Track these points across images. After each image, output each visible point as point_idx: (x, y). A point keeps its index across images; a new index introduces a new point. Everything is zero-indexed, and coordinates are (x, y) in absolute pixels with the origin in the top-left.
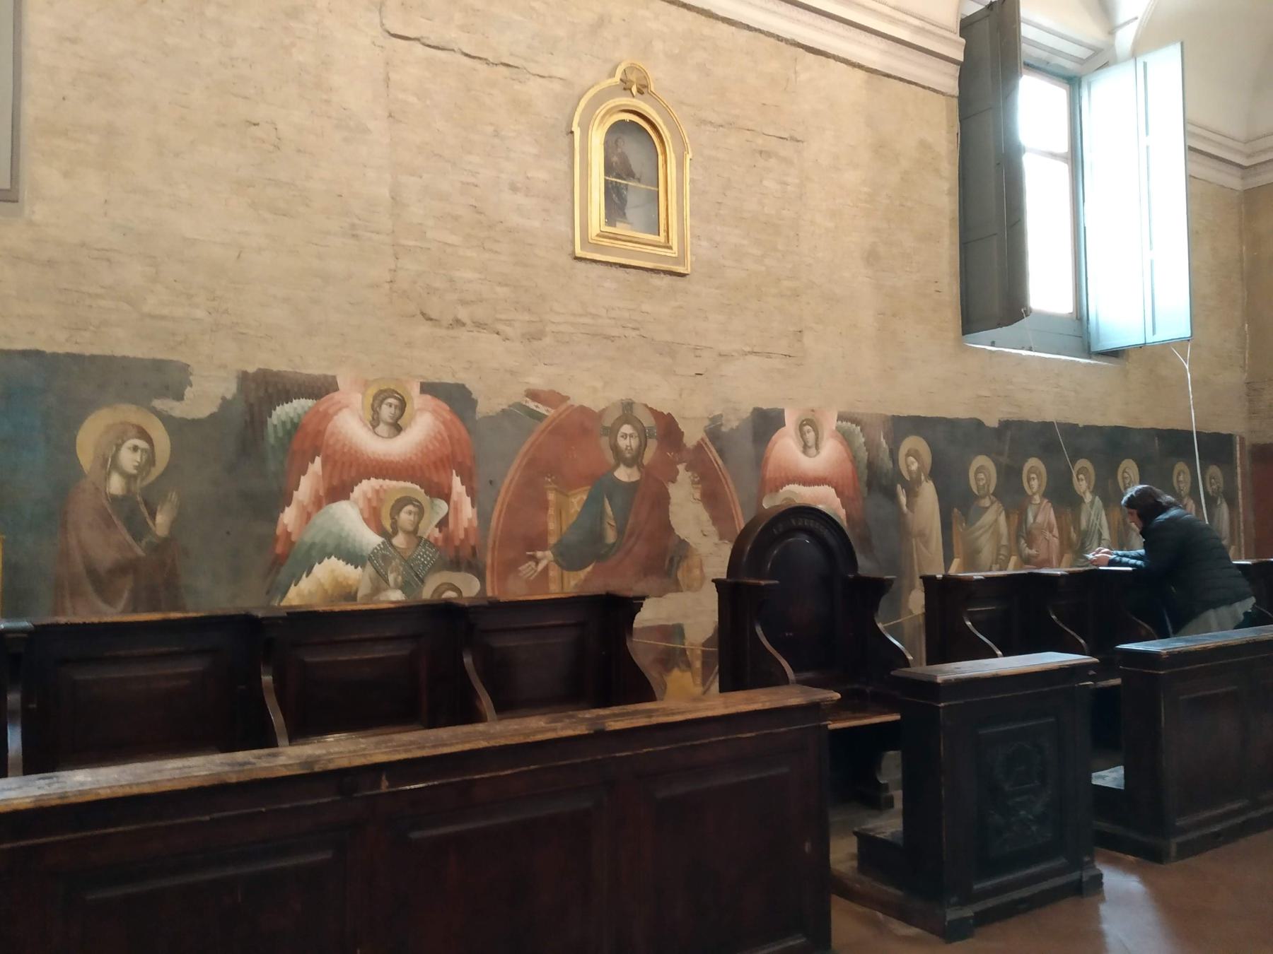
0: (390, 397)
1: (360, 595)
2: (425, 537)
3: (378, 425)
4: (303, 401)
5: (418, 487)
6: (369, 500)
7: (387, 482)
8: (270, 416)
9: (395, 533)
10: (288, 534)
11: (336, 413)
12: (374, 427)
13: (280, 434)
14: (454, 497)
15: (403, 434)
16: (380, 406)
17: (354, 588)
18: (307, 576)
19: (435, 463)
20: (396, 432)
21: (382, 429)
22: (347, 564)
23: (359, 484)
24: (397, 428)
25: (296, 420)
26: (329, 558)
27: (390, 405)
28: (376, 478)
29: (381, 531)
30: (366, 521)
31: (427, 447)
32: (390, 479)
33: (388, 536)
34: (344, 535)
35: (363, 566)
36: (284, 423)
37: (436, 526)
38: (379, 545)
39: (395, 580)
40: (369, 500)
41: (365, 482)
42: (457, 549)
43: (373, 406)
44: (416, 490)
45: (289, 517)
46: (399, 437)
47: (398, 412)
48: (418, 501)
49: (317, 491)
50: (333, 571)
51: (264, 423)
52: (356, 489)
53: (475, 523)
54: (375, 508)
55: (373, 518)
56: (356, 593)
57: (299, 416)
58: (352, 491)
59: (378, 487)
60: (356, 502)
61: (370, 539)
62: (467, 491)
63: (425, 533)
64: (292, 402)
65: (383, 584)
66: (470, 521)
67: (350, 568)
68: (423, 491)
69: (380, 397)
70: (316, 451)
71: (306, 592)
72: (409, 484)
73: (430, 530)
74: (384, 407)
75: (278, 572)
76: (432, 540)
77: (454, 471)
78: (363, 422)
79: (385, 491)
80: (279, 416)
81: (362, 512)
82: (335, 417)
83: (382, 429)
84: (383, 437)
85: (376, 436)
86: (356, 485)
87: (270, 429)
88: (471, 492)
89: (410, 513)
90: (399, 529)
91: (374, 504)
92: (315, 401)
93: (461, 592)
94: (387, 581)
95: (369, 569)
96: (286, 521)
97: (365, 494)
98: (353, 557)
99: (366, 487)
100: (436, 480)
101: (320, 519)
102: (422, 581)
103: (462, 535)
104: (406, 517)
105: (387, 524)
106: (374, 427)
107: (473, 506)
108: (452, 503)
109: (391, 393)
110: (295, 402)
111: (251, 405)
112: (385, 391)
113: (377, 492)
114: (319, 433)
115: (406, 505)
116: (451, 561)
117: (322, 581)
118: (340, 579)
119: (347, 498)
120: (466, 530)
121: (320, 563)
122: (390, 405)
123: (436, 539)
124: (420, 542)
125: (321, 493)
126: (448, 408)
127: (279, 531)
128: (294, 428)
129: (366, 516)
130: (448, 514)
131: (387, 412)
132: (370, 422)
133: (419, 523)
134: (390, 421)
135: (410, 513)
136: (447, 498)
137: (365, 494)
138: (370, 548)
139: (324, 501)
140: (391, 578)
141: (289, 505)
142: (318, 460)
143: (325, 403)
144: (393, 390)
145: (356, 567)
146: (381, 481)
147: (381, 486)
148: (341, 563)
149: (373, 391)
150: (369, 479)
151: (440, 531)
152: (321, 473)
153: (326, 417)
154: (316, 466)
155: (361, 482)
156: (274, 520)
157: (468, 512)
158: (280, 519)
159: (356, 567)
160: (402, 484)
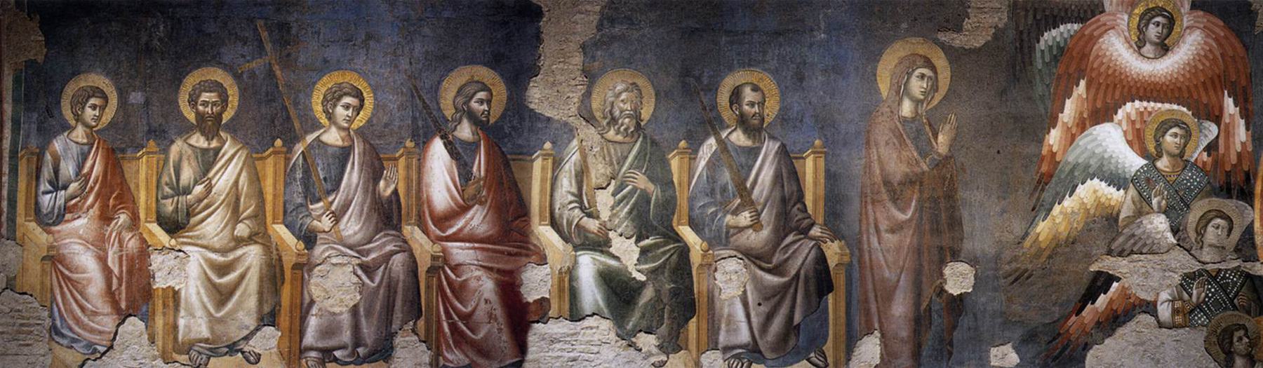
0: (1158, 15)
1: (1122, 216)
2: (1193, 160)
3: (1144, 45)
4: (1069, 26)
5: (1185, 109)
6: (1133, 122)
7: (1152, 104)
8: (1038, 42)
9: (1160, 156)
10: (1053, 155)
11: (1100, 36)
12: (1140, 48)
13: (1047, 60)
14: (1226, 119)
15: (1170, 53)
16: (1147, 25)
17: (1116, 209)
18: (1070, 196)
19: (1204, 83)
20: (1162, 53)
21: (1148, 49)
22: (1109, 185)
23: (1123, 107)
24: (1164, 48)
25: (1062, 45)
26: (1091, 179)
27: (1158, 24)
28: (1141, 100)
29: (1143, 153)
30: (1130, 143)
31: (1195, 67)
32: (1155, 101)
33: (1152, 159)
34: (1106, 156)
35: (1126, 189)
36: (1051, 48)
37: (1204, 150)
38: (1142, 167)
39: (1159, 203)
40: (1133, 122)
41: (1129, 105)
42: (1228, 174)
43: (1139, 25)
44: (1183, 112)
45: (1054, 138)
46: (1164, 57)
47: (1165, 31)
48: (1185, 124)
49: (1081, 113)
50: (1095, 191)
51: (1032, 49)
52: (1120, 111)
53: (1250, 149)
54: (1138, 130)
55: (1136, 140)
56: (1118, 215)
57: (1065, 40)
58: (1116, 114)
59: (1142, 110)
60: (1120, 123)
61: (1133, 162)
62: (1240, 112)
63: (1192, 157)
64: (1058, 27)
65: (1147, 208)
66: (1243, 144)
67: (1112, 190)
68: (1190, 113)
69: (1147, 17)
70: (1081, 74)
71: (1069, 210)
72: (1175, 107)
73: (1198, 153)
74: (1151, 26)
75: (1043, 190)
76: (1200, 165)
77: (1226, 92)
78: (1129, 43)
79: (1150, 113)
80: (1046, 41)
81: (1125, 133)
82: (1101, 40)
83: (1148, 49)
84: (1148, 58)
85: (1142, 58)
86: (1120, 108)
87: (1038, 55)
88: (1245, 114)
89: (1175, 135)
90: (1164, 152)
91: (1138, 126)
92: (1081, 25)
93: (1231, 221)
94: (1150, 204)
95: (1132, 191)
96: (1051, 143)
97: (1128, 116)
98: (1116, 180)
99: (1130, 108)
100: (1205, 100)
101: (1083, 141)
102: (1188, 207)
103: (1234, 160)
104: (1171, 140)
105: (1151, 147)
106: (1140, 48)
107: (1247, 129)
108: (1222, 126)
109: (1160, 11)
110: (1062, 28)
111: (1021, 32)
112: (1153, 9)
113: (1142, 113)
114: (1084, 56)
115: (1171, 128)
116: (1221, 188)
117: (1085, 201)
118: (1103, 200)
119: (1111, 120)
120: (1239, 155)
121: (1082, 184)
122: (1158, 24)
123: (1204, 163)
124: (1186, 166)
125: (1085, 116)
126: (1221, 23)
127: (1045, 151)
128: (1060, 52)
129: (1130, 138)
130: (1217, 137)
131: (1153, 32)
132: (1136, 43)
133: (1185, 146)
134: (1158, 41)
135: (1175, 135)
136: (1217, 120)
137: (1128, 116)
138: (1133, 170)
139: (1087, 123)
140: (1155, 201)
141: (1054, 128)
142: (1083, 83)
143: (1090, 28)
144: (1162, 8)
145: (1118, 190)
146: (1145, 104)
147: (1145, 108)
148: (1103, 184)
149: (1139, 11)
150: (1133, 101)
151: (1209, 155)
152: (1085, 96)
153: (1093, 40)
154: (1081, 89)
155: (1125, 104)
156: (1041, 141)
157: (1241, 134)
158: (1046, 140)
159: (1118, 190)
160: (1167, 106)
